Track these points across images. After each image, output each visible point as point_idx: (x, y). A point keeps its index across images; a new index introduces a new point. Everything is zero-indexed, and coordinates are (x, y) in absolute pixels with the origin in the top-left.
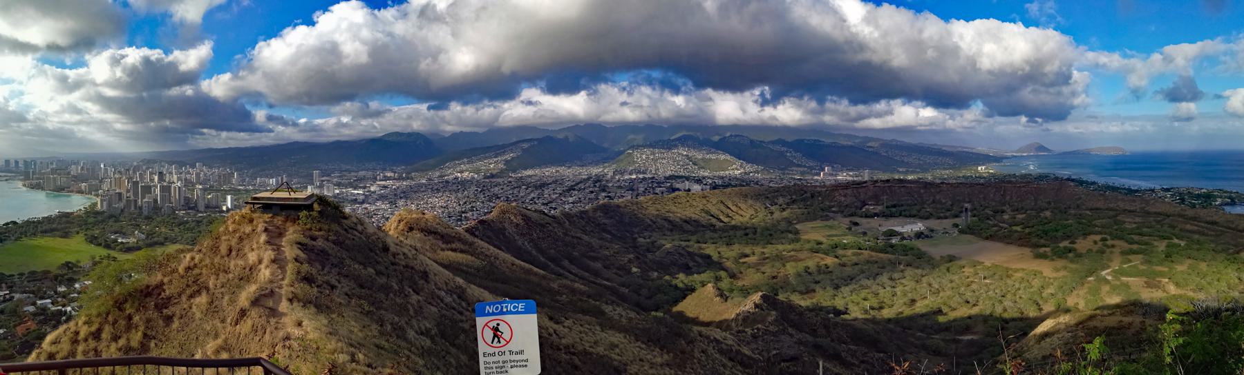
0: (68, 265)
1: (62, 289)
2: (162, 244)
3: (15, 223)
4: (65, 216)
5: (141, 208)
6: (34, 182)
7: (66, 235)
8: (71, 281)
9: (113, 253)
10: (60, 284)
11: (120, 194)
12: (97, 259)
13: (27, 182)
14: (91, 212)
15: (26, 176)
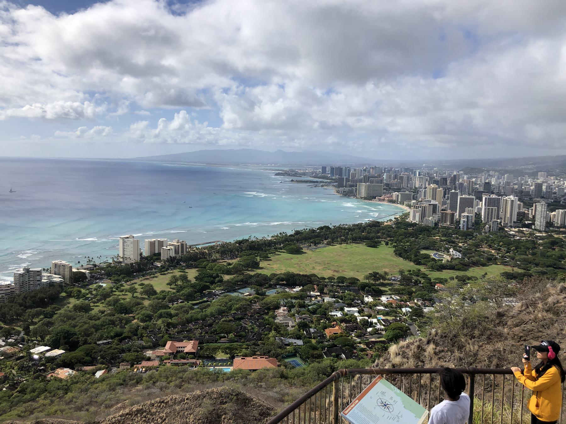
0: (375, 276)
1: (369, 299)
2: (484, 265)
3: (328, 228)
4: (376, 225)
5: (458, 222)
6: (347, 189)
7: (374, 244)
8: (377, 294)
9: (423, 269)
10: (368, 293)
11: (435, 206)
12: (406, 273)
13: (341, 189)
14: (402, 223)
15: (339, 183)
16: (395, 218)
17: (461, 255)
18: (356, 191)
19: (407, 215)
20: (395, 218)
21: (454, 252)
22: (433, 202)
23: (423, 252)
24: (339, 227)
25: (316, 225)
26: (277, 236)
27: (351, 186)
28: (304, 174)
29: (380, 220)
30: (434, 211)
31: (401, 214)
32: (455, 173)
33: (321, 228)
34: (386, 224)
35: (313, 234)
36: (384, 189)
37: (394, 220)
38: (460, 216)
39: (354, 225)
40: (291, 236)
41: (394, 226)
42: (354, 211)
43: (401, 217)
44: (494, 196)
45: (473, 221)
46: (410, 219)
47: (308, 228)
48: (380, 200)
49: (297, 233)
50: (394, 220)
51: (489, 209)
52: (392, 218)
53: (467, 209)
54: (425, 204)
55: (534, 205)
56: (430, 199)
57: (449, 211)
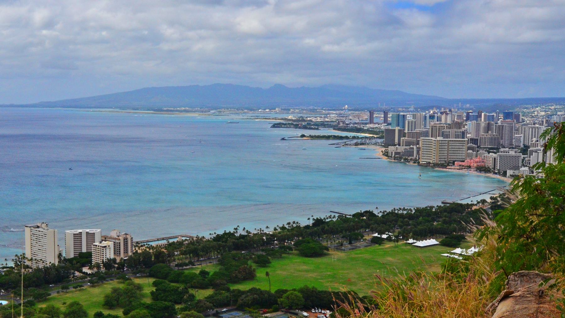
3: (370, 214)
6: (401, 149)
13: (391, 149)
16: (491, 198)
20: (491, 198)
24: (392, 213)
25: (350, 211)
26: (283, 228)
27: (408, 144)
29: (464, 202)
34: (474, 208)
35: (345, 225)
36: (469, 148)
37: (489, 200)
39: (417, 210)
40: (307, 227)
42: (414, 190)
47: (337, 215)
48: (462, 167)
49: (318, 222)
50: (489, 200)
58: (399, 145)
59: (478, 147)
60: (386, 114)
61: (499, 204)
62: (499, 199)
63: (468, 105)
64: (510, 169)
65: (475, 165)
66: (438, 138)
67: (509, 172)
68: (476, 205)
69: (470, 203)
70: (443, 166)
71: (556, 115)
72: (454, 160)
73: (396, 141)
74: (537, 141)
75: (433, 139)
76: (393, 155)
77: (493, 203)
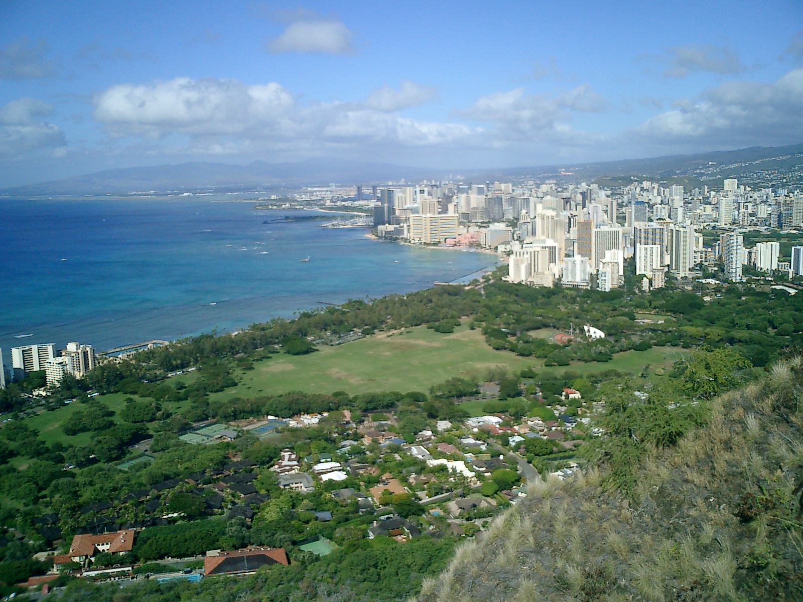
3: (360, 303)
8: (459, 417)
11: (552, 250)
17: (603, 335)
18: (409, 230)
19: (505, 270)
21: (593, 330)
22: (550, 243)
23: (533, 334)
25: (339, 302)
28: (308, 203)
30: (552, 260)
31: (495, 270)
32: (584, 186)
33: (351, 303)
34: (467, 288)
37: (482, 280)
38: (597, 265)
40: (293, 322)
41: (483, 292)
43: (494, 273)
44: (655, 225)
45: (621, 272)
46: (512, 277)
47: (324, 307)
51: (646, 249)
52: (479, 276)
53: (608, 253)
54: (536, 247)
55: (721, 235)
56: (543, 238)
57: (578, 258)
58: (389, 224)
59: (469, 222)
60: (374, 188)
61: (491, 282)
62: (491, 278)
63: (459, 177)
64: (502, 244)
65: (467, 241)
66: (429, 215)
67: (501, 248)
68: (468, 285)
69: (462, 284)
70: (435, 244)
71: (544, 184)
72: (446, 237)
73: (386, 219)
74: (527, 213)
75: (424, 216)
76: (384, 235)
77: (485, 282)
